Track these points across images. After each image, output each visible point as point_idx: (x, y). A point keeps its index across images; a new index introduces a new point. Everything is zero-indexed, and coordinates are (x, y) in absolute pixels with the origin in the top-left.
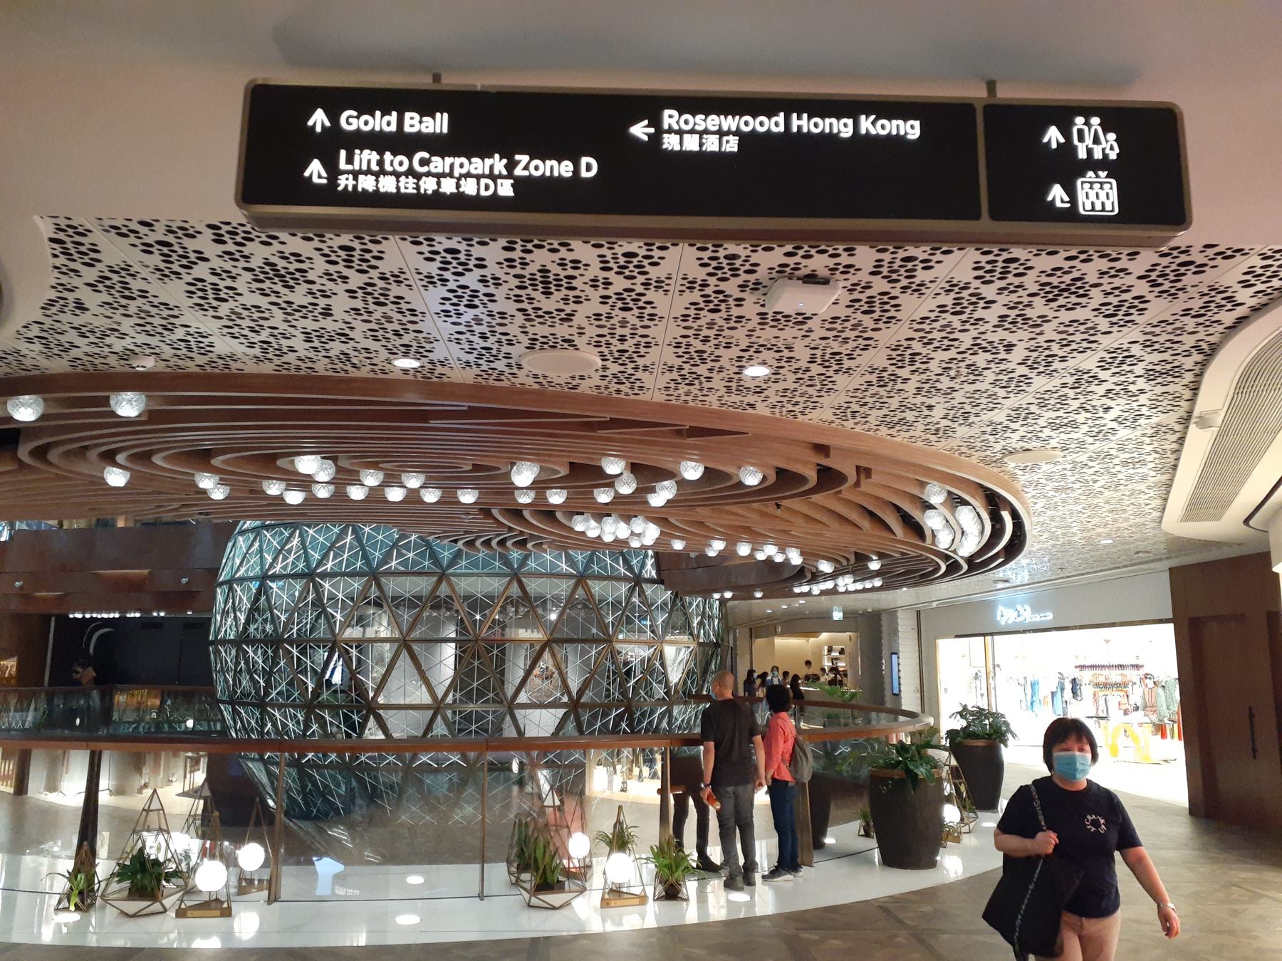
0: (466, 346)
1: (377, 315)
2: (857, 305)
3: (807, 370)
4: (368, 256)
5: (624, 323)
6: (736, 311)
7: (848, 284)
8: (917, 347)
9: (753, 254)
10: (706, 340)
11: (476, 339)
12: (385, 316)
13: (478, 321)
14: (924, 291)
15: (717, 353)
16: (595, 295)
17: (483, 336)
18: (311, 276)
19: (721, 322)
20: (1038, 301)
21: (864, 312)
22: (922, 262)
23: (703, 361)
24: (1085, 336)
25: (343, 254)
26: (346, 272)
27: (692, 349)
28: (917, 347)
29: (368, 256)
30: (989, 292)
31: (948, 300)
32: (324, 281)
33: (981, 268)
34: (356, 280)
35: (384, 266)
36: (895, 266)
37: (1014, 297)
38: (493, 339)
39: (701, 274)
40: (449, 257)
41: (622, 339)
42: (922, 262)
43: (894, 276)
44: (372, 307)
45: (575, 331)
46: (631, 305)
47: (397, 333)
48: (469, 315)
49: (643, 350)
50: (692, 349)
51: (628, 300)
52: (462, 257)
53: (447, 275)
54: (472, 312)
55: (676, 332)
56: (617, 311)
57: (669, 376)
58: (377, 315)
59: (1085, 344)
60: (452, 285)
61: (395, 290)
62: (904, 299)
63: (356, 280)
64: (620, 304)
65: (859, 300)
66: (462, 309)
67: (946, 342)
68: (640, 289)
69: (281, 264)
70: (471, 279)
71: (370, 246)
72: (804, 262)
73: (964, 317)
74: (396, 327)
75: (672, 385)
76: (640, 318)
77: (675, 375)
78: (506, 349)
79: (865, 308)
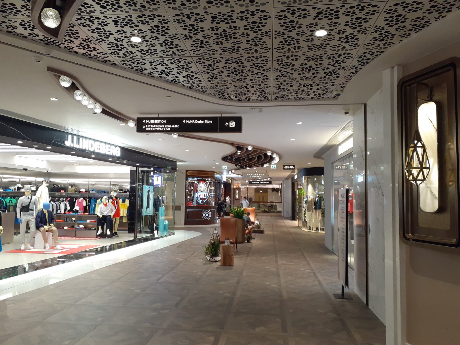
0: (216, 90)
1: (191, 82)
4: (188, 67)
5: (259, 81)
7: (322, 68)
10: (284, 85)
11: (218, 87)
12: (193, 82)
13: (218, 83)
15: (288, 88)
17: (220, 87)
18: (173, 73)
23: (285, 91)
25: (181, 67)
26: (182, 72)
27: (281, 88)
29: (188, 67)
32: (177, 74)
34: (185, 73)
35: (192, 70)
36: (334, 63)
38: (223, 87)
40: (209, 67)
41: (260, 86)
43: (335, 65)
44: (189, 80)
47: (196, 87)
48: (215, 81)
49: (266, 88)
50: (281, 88)
52: (213, 67)
53: (209, 71)
54: (216, 80)
56: (256, 78)
57: (275, 95)
58: (191, 82)
60: (210, 74)
61: (195, 76)
63: (185, 73)
64: (257, 76)
66: (213, 80)
68: (262, 72)
69: (166, 70)
70: (215, 72)
71: (188, 65)
72: (308, 63)
74: (196, 85)
75: (277, 98)
76: (264, 79)
77: (277, 95)
78: (226, 90)
79: (329, 74)
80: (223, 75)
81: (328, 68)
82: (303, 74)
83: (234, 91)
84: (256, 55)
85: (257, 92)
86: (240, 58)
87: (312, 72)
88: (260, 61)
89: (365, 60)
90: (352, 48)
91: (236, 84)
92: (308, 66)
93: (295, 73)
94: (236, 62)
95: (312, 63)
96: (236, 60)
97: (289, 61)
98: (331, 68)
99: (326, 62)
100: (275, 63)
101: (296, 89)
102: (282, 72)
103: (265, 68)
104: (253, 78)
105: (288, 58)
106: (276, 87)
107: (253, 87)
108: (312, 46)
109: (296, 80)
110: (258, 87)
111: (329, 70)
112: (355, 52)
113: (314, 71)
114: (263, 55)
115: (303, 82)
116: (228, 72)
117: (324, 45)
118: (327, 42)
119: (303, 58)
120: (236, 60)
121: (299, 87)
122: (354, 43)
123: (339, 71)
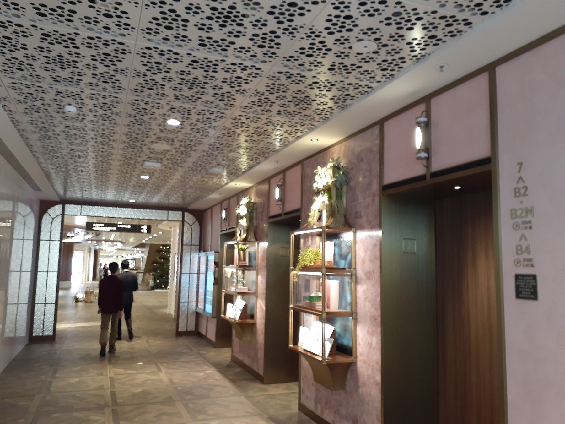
2: (217, 96)
3: (196, 125)
5: (105, 89)
8: (244, 120)
9: (168, 63)
10: (147, 103)
14: (245, 94)
15: (153, 110)
16: (89, 73)
19: (154, 95)
20: (292, 105)
21: (220, 100)
22: (245, 80)
24: (310, 122)
27: (140, 107)
28: (244, 120)
30: (272, 98)
31: (255, 99)
33: (269, 86)
36: (233, 80)
37: (282, 102)
39: (143, 69)
42: (245, 80)
43: (233, 85)
46: (108, 80)
51: (107, 78)
55: (132, 97)
59: (310, 126)
62: (238, 96)
64: (102, 79)
65: (217, 94)
67: (255, 119)
73: (262, 108)
75: (131, 124)
77: (132, 119)
79: (220, 98)
80: (36, 65)
82: (181, 90)
83: (55, 100)
84: (105, 36)
85: (97, 109)
86: (73, 36)
87: (195, 90)
88: (110, 50)
89: (277, 86)
90: (267, 59)
91: (61, 87)
92: (191, 77)
93: (168, 85)
94: (64, 44)
95: (199, 73)
96: (64, 38)
97: (163, 60)
98: (226, 88)
99: (221, 75)
101: (164, 115)
102: (147, 78)
103: (119, 65)
104: (94, 81)
106: (133, 104)
107: (91, 99)
108: (207, 40)
109: (168, 99)
110: (102, 100)
111: (222, 91)
112: (270, 68)
113: (199, 89)
114: (120, 39)
115: (177, 104)
116: (45, 60)
117: (226, 43)
118: (233, 39)
119: (188, 60)
120: (64, 38)
121: (170, 112)
122: (272, 50)
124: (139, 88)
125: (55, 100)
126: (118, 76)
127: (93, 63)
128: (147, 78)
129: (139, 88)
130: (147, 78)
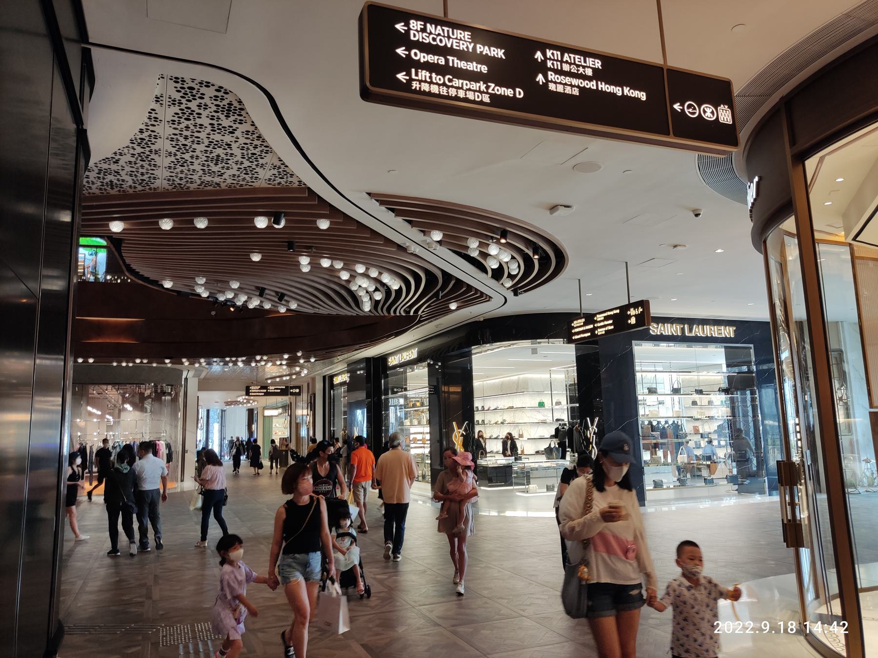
5: (142, 167)
6: (191, 167)
41: (142, 174)
45: (120, 168)
76: (150, 165)
81: (242, 163)
93: (196, 162)
100: (168, 142)
104: (133, 160)
105: (186, 138)
106: (169, 180)
123: (258, 170)
124: (172, 165)
125: (99, 178)
126: (153, 156)
127: (131, 145)
128: (178, 157)
129: (172, 165)
130: (178, 157)
